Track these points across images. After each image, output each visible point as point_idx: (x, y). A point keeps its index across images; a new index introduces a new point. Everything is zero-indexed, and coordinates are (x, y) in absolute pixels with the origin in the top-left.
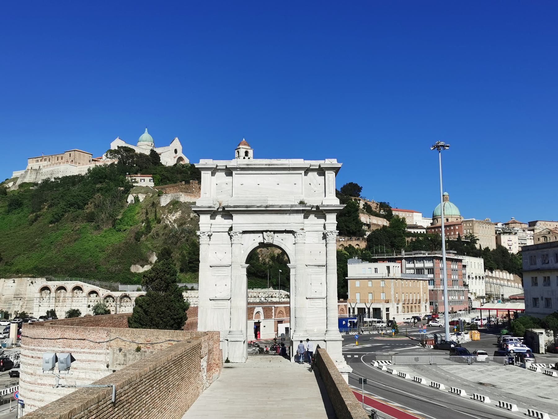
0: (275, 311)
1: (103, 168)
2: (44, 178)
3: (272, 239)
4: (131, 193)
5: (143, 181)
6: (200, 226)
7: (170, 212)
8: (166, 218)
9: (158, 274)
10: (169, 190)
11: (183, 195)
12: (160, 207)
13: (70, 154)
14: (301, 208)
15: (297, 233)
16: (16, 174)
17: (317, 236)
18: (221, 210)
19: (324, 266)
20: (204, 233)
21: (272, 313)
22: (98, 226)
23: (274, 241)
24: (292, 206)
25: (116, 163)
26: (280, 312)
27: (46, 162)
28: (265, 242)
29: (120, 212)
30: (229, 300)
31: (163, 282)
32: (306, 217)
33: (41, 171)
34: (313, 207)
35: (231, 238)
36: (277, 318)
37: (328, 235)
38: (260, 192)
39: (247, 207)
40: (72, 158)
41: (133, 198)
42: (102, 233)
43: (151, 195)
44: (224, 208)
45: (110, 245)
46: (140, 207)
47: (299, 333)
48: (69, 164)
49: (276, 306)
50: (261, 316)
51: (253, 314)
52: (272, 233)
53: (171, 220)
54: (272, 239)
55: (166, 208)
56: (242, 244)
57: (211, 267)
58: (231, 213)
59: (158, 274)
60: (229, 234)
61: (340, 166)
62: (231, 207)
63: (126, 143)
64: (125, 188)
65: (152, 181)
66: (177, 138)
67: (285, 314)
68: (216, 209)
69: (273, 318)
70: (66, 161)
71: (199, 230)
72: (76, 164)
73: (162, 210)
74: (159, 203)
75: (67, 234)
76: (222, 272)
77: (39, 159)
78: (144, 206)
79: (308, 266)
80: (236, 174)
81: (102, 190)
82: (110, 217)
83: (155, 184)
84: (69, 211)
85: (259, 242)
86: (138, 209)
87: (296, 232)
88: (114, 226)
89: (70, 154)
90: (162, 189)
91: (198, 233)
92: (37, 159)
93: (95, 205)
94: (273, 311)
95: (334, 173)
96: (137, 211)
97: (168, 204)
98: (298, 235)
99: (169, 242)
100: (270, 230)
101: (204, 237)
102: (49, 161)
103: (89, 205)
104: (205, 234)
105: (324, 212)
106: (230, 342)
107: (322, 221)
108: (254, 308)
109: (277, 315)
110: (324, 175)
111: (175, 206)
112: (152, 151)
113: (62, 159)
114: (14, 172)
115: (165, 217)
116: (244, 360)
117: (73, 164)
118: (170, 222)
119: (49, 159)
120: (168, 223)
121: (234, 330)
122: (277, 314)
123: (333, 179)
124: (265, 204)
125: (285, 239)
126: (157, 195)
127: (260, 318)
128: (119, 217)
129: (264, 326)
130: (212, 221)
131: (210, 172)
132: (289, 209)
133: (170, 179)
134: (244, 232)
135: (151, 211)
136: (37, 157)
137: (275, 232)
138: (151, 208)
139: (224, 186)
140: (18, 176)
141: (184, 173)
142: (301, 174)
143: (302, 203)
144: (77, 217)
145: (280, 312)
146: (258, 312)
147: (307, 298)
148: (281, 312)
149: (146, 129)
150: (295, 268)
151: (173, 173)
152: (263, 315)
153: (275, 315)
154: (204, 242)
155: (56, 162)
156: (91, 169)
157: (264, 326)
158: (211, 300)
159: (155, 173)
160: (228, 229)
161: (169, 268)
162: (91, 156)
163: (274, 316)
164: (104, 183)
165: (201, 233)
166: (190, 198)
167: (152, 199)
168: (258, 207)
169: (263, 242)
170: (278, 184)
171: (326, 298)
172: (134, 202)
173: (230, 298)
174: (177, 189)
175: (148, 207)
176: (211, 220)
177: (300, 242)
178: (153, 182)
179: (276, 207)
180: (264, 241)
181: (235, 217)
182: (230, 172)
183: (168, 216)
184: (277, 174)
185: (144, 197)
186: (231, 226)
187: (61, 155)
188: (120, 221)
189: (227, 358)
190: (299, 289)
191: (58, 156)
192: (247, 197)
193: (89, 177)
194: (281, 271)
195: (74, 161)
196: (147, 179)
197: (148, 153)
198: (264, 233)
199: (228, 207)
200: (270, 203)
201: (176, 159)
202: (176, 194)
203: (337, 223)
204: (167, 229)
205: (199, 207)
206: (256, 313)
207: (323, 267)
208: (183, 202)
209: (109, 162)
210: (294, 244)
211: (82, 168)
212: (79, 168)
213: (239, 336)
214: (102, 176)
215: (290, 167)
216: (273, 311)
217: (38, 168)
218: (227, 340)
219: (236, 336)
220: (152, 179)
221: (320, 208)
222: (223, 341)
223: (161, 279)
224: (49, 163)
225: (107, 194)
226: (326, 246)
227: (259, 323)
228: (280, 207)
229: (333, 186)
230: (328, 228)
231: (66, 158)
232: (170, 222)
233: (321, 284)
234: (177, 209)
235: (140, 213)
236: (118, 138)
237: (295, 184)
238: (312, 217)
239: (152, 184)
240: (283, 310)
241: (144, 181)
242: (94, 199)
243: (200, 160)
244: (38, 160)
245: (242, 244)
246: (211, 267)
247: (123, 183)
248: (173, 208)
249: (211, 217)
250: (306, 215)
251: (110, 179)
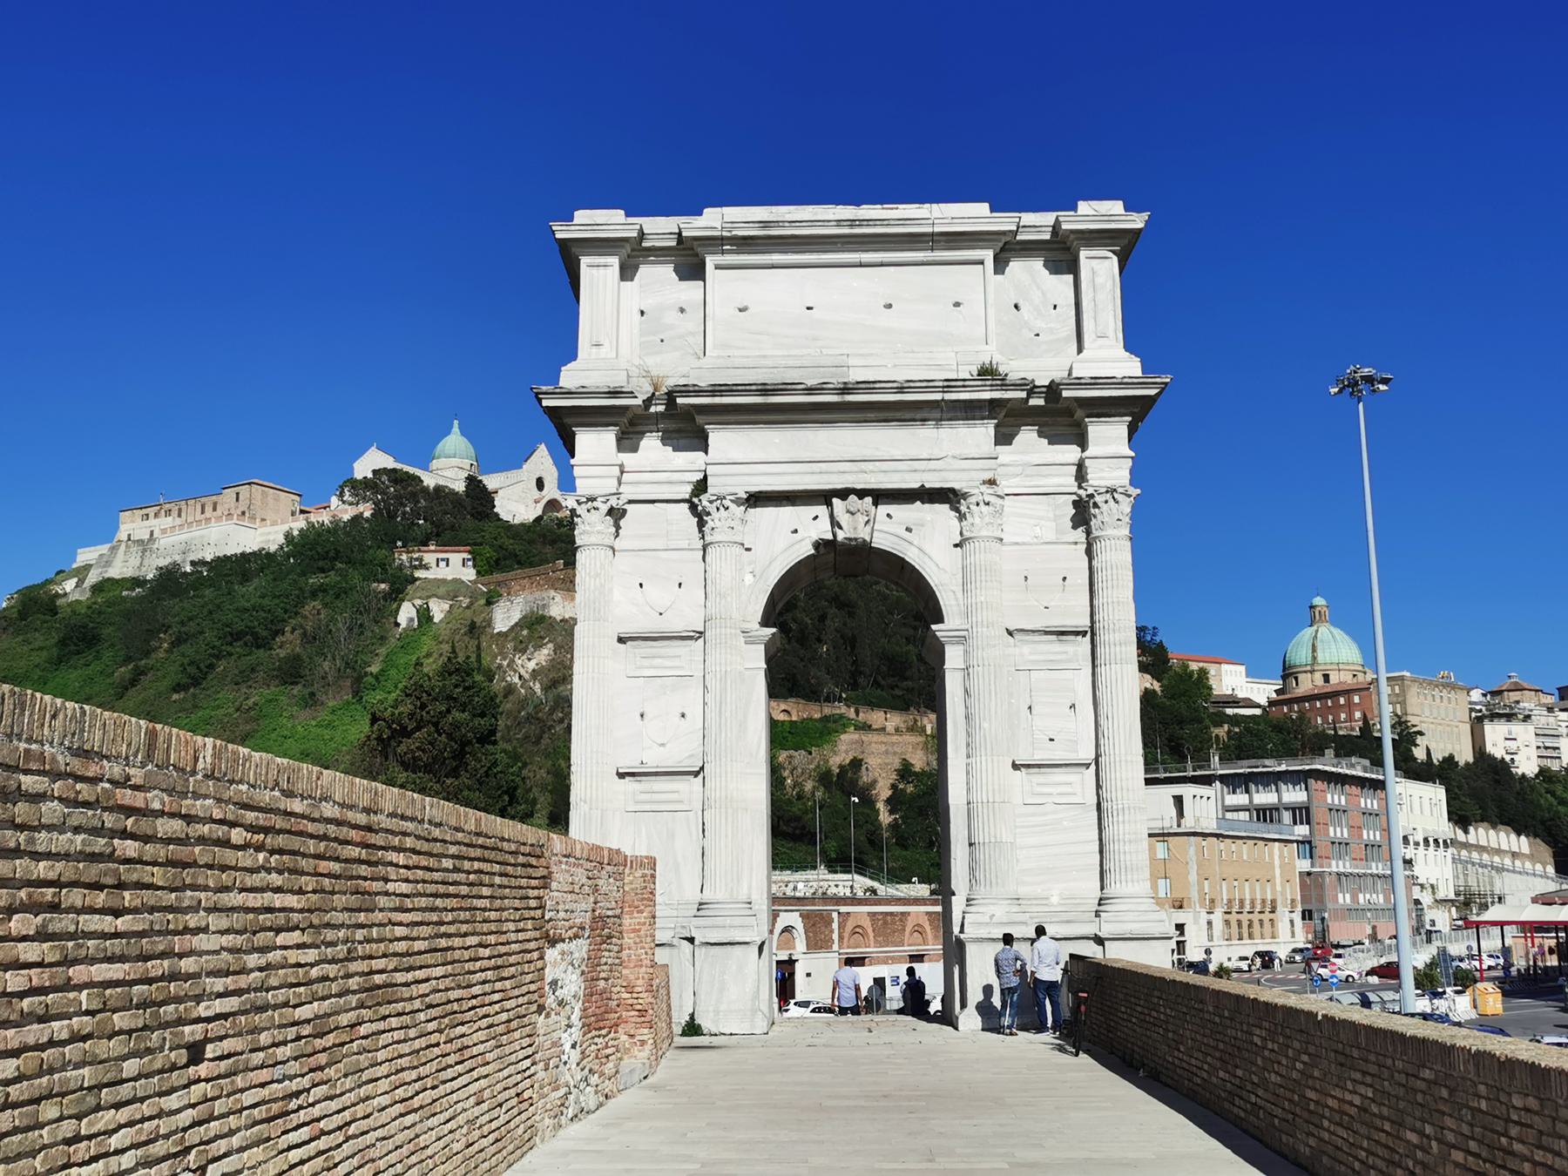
0: (842, 926)
1: (329, 531)
2: (164, 562)
3: (868, 528)
4: (408, 597)
5: (443, 564)
6: (577, 472)
7: (520, 647)
8: (508, 665)
9: (423, 706)
10: (518, 588)
11: (558, 598)
12: (493, 636)
13: (238, 494)
14: (987, 395)
15: (972, 500)
16: (85, 556)
17: (1051, 515)
18: (661, 408)
19: (1084, 634)
20: (592, 499)
21: (832, 931)
22: (312, 694)
23: (875, 534)
24: (949, 384)
25: (367, 514)
26: (857, 930)
27: (170, 519)
28: (841, 536)
29: (377, 655)
30: (696, 774)
31: (443, 738)
32: (1004, 437)
33: (156, 546)
34: (1032, 390)
35: (701, 524)
36: (848, 947)
37: (1096, 505)
38: (815, 339)
39: (765, 390)
40: (243, 506)
41: (414, 613)
42: (324, 715)
43: (466, 602)
44: (671, 396)
45: (344, 748)
46: (435, 638)
47: (990, 910)
48: (235, 521)
49: (843, 909)
50: (797, 942)
52: (869, 500)
53: (522, 672)
54: (868, 528)
55: (510, 638)
56: (748, 550)
57: (621, 640)
58: (700, 419)
59: (423, 706)
60: (693, 508)
61: (1140, 225)
62: (699, 392)
63: (397, 460)
64: (392, 584)
65: (470, 563)
66: (543, 447)
67: (871, 938)
68: (638, 402)
69: (835, 947)
70: (226, 513)
72: (255, 523)
73: (497, 645)
74: (489, 623)
75: (221, 721)
76: (667, 663)
77: (151, 511)
78: (445, 634)
79: (1018, 636)
80: (718, 267)
81: (325, 591)
82: (346, 668)
83: (478, 573)
84: (230, 654)
85: (815, 537)
86: (427, 644)
87: (965, 496)
88: (357, 693)
89: (238, 494)
90: (499, 584)
92: (145, 511)
93: (304, 634)
94: (835, 926)
95: (1115, 259)
96: (425, 649)
97: (516, 624)
98: (973, 507)
99: (518, 736)
100: (859, 487)
101: (594, 515)
102: (179, 516)
103: (288, 634)
104: (595, 504)
105: (1079, 413)
106: (704, 949)
107: (1071, 453)
109: (846, 940)
110: (1072, 267)
111: (536, 629)
112: (472, 482)
113: (215, 509)
114: (79, 551)
115: (505, 663)
116: (761, 1026)
117: (244, 521)
118: (520, 677)
119: (180, 510)
120: (516, 680)
121: (719, 896)
122: (846, 935)
123: (1110, 283)
124: (836, 380)
125: (922, 525)
126: (483, 602)
127: (794, 948)
128: (374, 669)
129: (808, 975)
130: (627, 458)
131: (614, 261)
132: (938, 397)
133: (524, 558)
134: (757, 499)
135: (467, 647)
136: (144, 504)
137: (881, 496)
138: (466, 639)
139: (672, 317)
140: (91, 562)
141: (563, 541)
142: (981, 263)
143: (988, 373)
144: (253, 670)
145: (857, 930)
146: (788, 929)
147: (1015, 766)
148: (861, 931)
149: (456, 422)
150: (962, 640)
151: (531, 542)
152: (804, 936)
153: (841, 938)
154: (593, 539)
155: (199, 516)
156: (296, 533)
158: (621, 776)
159: (479, 540)
160: (689, 488)
161: (467, 689)
162: (298, 498)
163: (836, 941)
164: (332, 573)
165: (579, 503)
167: (468, 612)
168: (810, 390)
169: (830, 537)
170: (889, 306)
171: (1093, 767)
172: (416, 623)
173: (702, 768)
174: (541, 582)
175: (457, 638)
176: (620, 455)
177: (984, 533)
178: (474, 566)
179: (883, 390)
180: (834, 535)
181: (723, 440)
182: (695, 260)
183: (516, 659)
184: (882, 265)
185: (447, 607)
186: (700, 476)
187: (214, 497)
188: (377, 678)
189: (692, 1016)
190: (985, 725)
191: (203, 500)
192: (764, 356)
193: (288, 556)
194: (857, 800)
195: (247, 515)
196: (456, 558)
197: (460, 487)
198: (835, 501)
199: (687, 390)
201: (540, 506)
202: (537, 594)
203: (1133, 454)
204: (511, 698)
205: (569, 393)
206: (783, 932)
207: (1079, 638)
208: (558, 618)
209: (347, 514)
210: (956, 546)
211: (269, 533)
212: (261, 535)
213: (738, 921)
214: (327, 552)
215: (937, 229)
216: (835, 926)
217: (148, 537)
218: (691, 940)
219: (728, 921)
220: (469, 560)
221: (1065, 394)
222: (671, 945)
223: (436, 725)
224: (178, 521)
225: (339, 604)
226: (1089, 552)
227: (791, 962)
228: (901, 390)
229: (1111, 307)
230: (1099, 476)
231: (227, 506)
232: (520, 677)
233: (1073, 706)
234: (542, 638)
235: (435, 656)
236: (373, 448)
237: (957, 304)
238: (1028, 437)
239: (469, 574)
240: (867, 923)
241: (447, 565)
242: (302, 617)
243: (576, 213)
244: (147, 515)
245: (748, 550)
246: (621, 640)
247: (385, 570)
248: (530, 638)
249: (619, 440)
250: (1003, 430)
251: (349, 562)
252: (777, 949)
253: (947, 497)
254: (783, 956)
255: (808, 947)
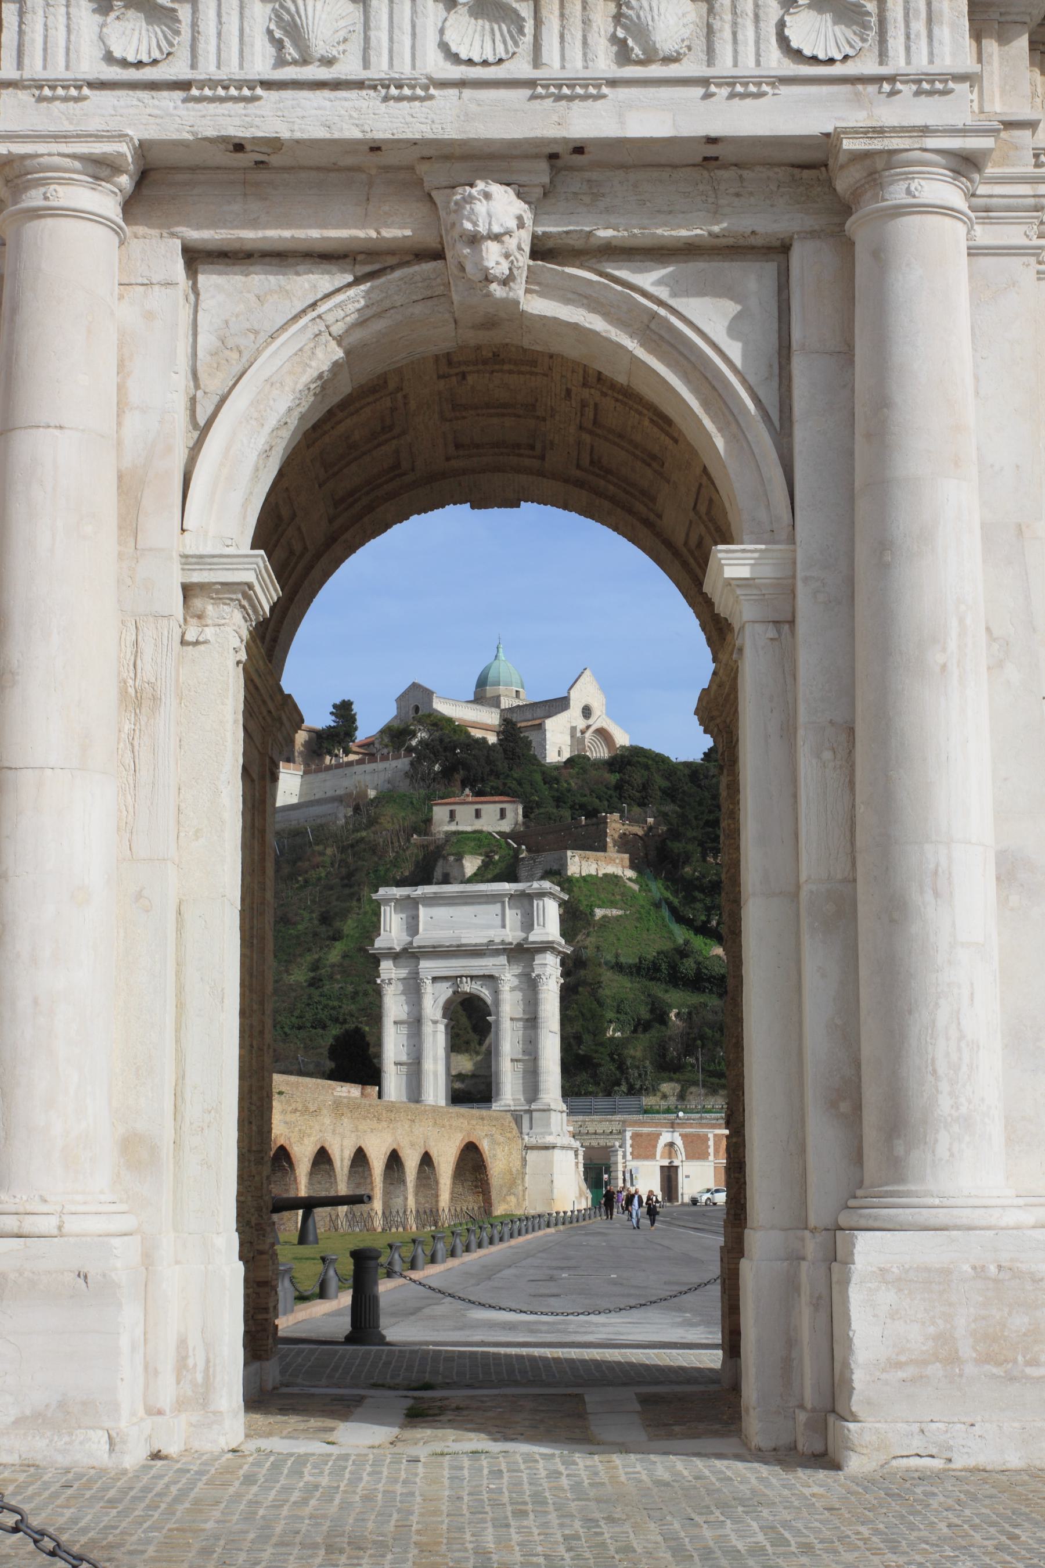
21: (708, 1147)
39: (434, 947)
51: (655, 1147)
69: (711, 1158)
71: (379, 976)
91: (379, 981)
94: (711, 1143)
108: (659, 1135)
124: (454, 943)
129: (688, 1177)
146: (671, 1145)
157: (688, 1177)
163: (712, 1154)
166: (594, 866)
200: (464, 941)
216: (711, 1143)
252: (662, 1157)
253: (491, 977)
254: (666, 1163)
255: (687, 1158)
